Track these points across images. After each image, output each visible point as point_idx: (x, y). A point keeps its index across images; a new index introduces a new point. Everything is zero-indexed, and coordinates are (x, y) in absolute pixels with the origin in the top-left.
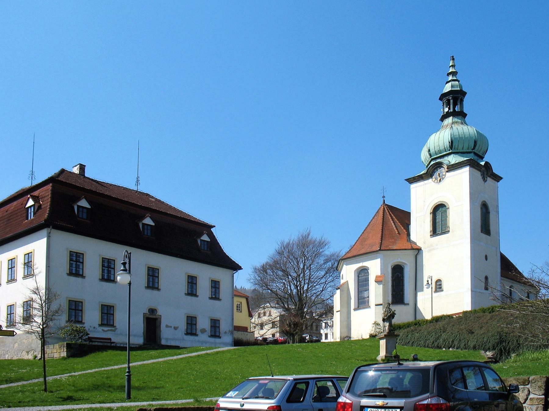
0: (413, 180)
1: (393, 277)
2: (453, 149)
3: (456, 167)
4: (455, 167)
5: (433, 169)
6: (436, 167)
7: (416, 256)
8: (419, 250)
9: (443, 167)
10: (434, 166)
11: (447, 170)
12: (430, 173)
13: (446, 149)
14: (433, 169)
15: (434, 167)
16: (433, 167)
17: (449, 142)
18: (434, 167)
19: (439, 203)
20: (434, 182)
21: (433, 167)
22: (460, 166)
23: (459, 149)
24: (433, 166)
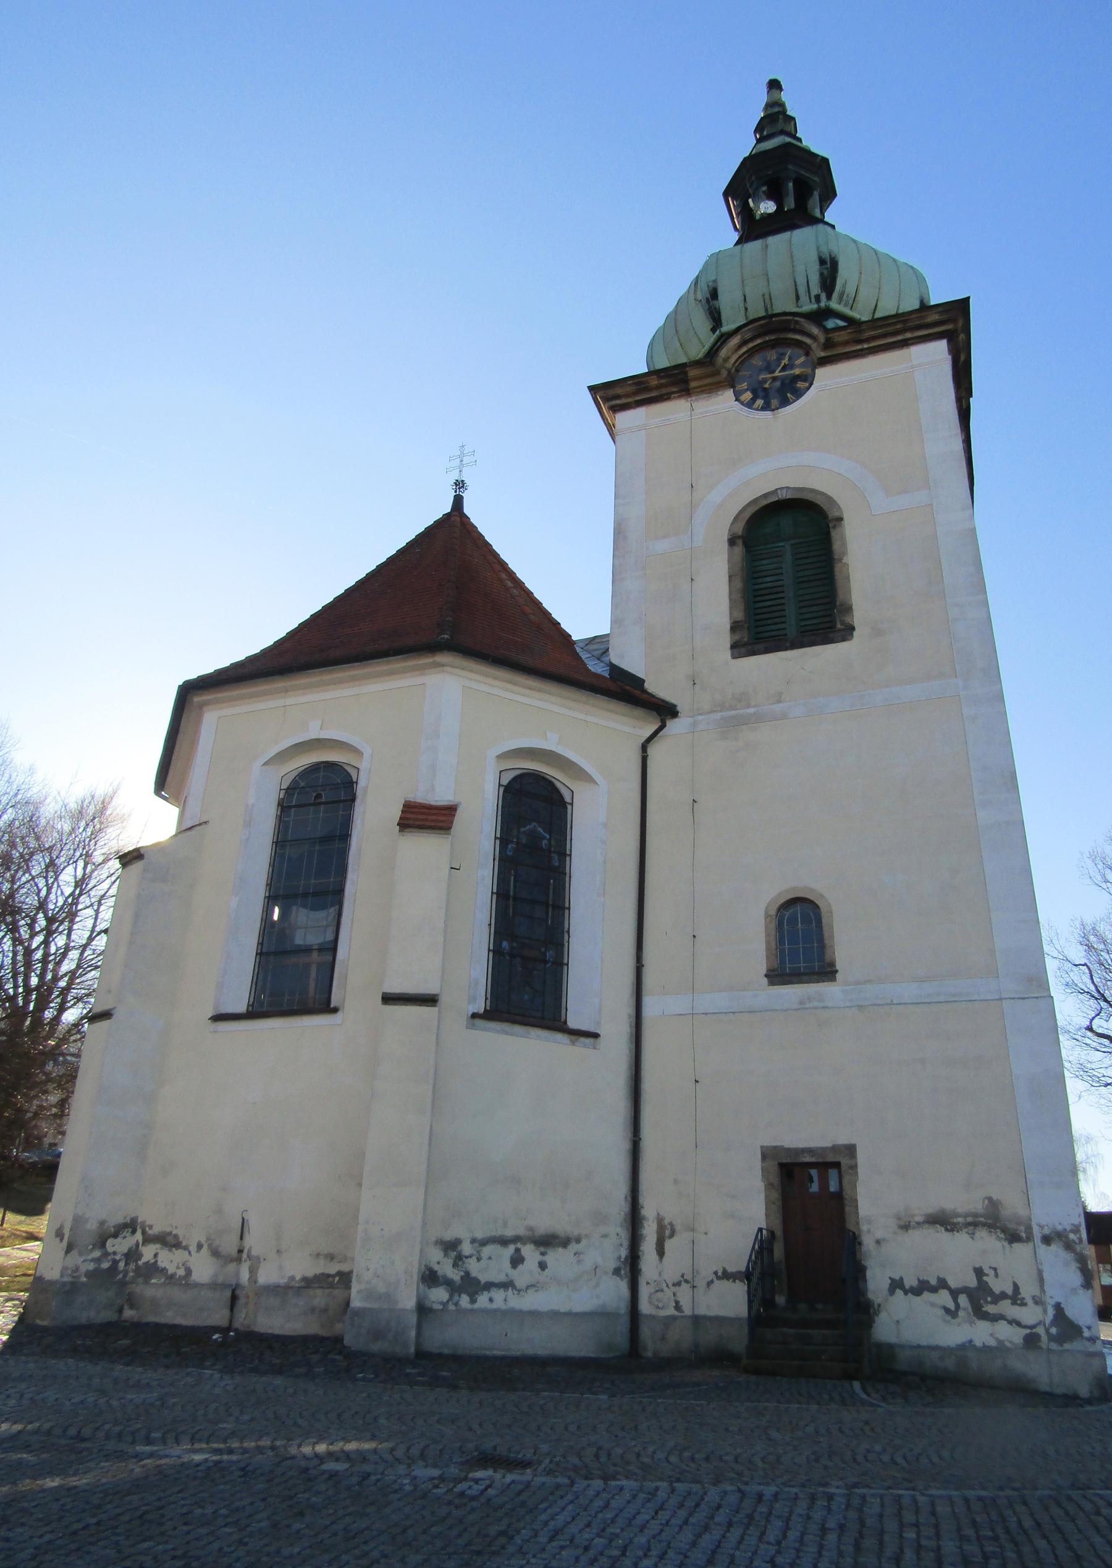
0: (635, 393)
1: (504, 839)
2: (835, 295)
3: (874, 338)
4: (868, 340)
5: (744, 349)
6: (759, 341)
7: (644, 747)
8: (665, 711)
9: (799, 344)
10: (751, 340)
11: (823, 354)
12: (729, 365)
13: (802, 290)
14: (744, 349)
15: (751, 345)
16: (744, 343)
17: (822, 262)
18: (751, 345)
19: (783, 495)
20: (750, 405)
21: (744, 343)
22: (900, 338)
23: (859, 305)
24: (748, 336)
